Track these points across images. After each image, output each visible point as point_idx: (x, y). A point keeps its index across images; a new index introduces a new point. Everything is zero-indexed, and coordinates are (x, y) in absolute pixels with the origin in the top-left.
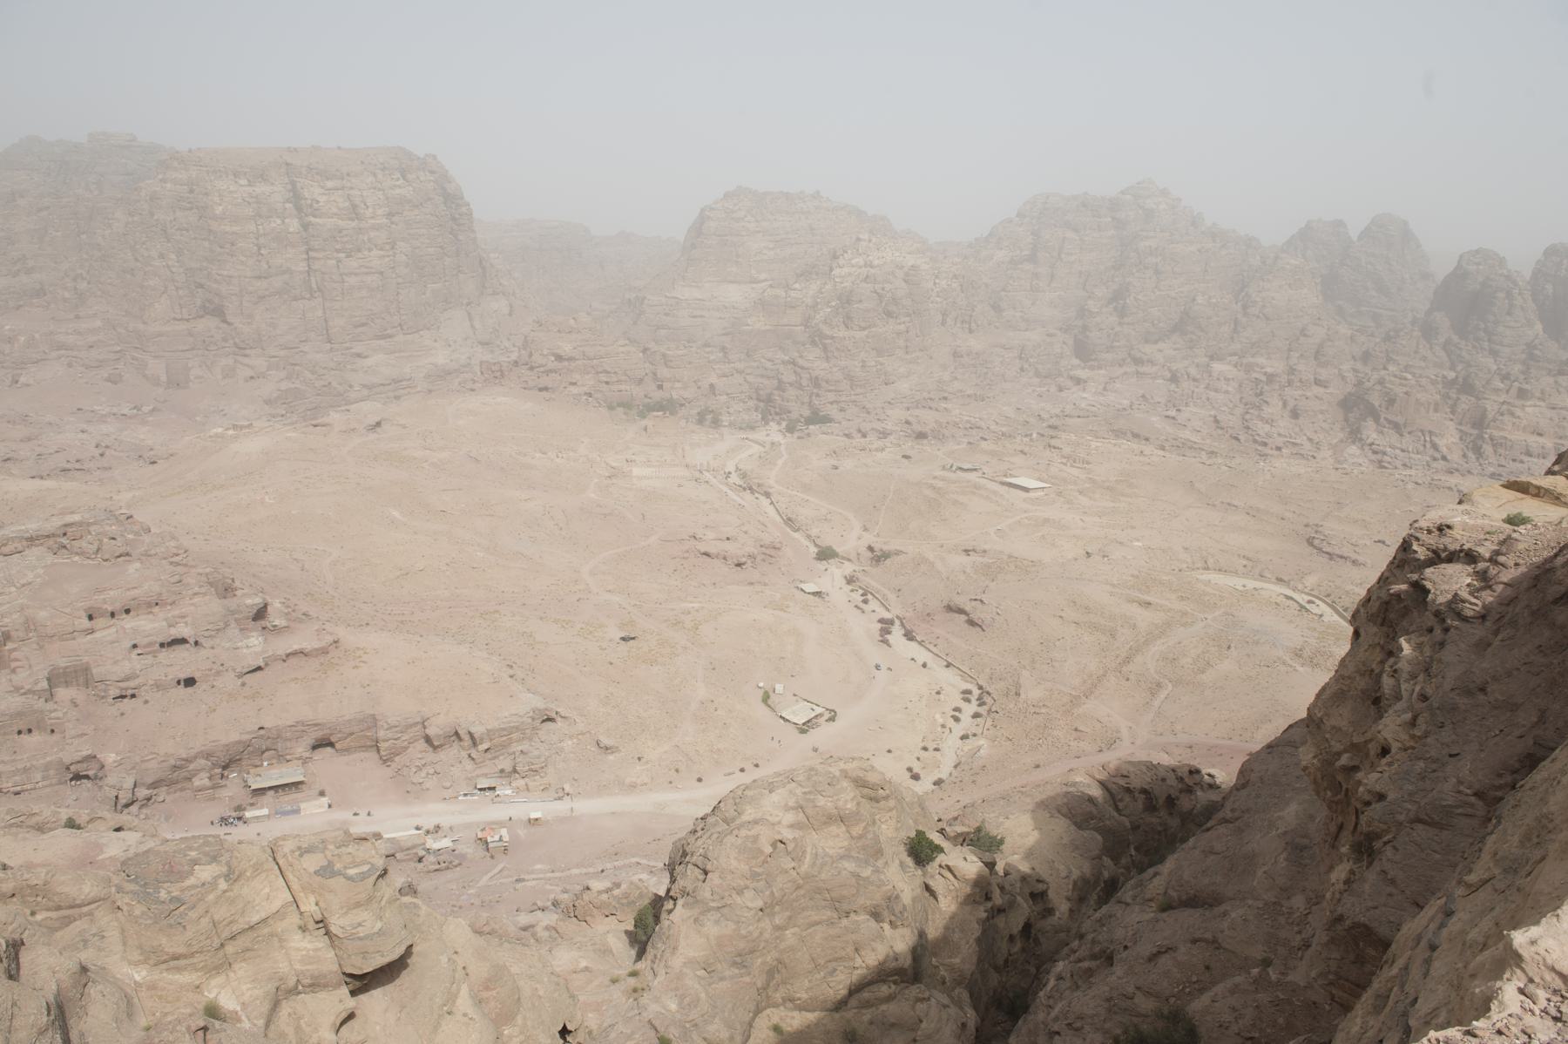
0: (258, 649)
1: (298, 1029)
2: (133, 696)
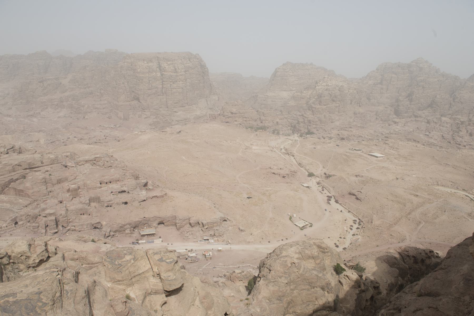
0: (145, 195)
1: (151, 305)
2: (111, 206)
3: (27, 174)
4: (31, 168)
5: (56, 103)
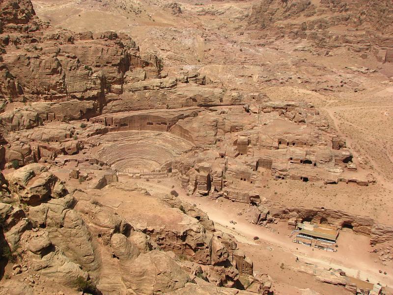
0: (337, 174)
2: (283, 178)
3: (200, 112)
4: (207, 105)
5: (296, 30)
